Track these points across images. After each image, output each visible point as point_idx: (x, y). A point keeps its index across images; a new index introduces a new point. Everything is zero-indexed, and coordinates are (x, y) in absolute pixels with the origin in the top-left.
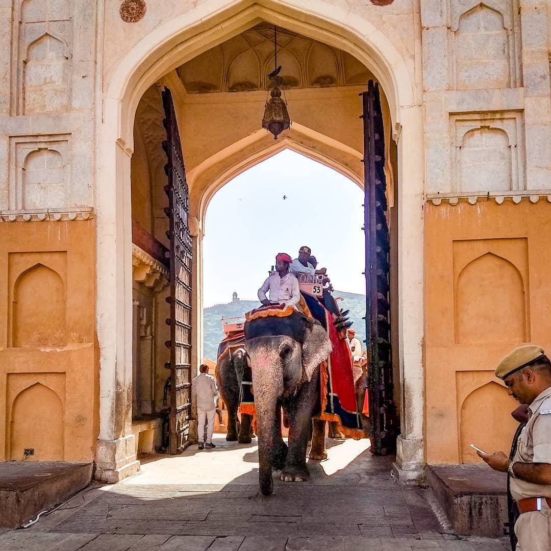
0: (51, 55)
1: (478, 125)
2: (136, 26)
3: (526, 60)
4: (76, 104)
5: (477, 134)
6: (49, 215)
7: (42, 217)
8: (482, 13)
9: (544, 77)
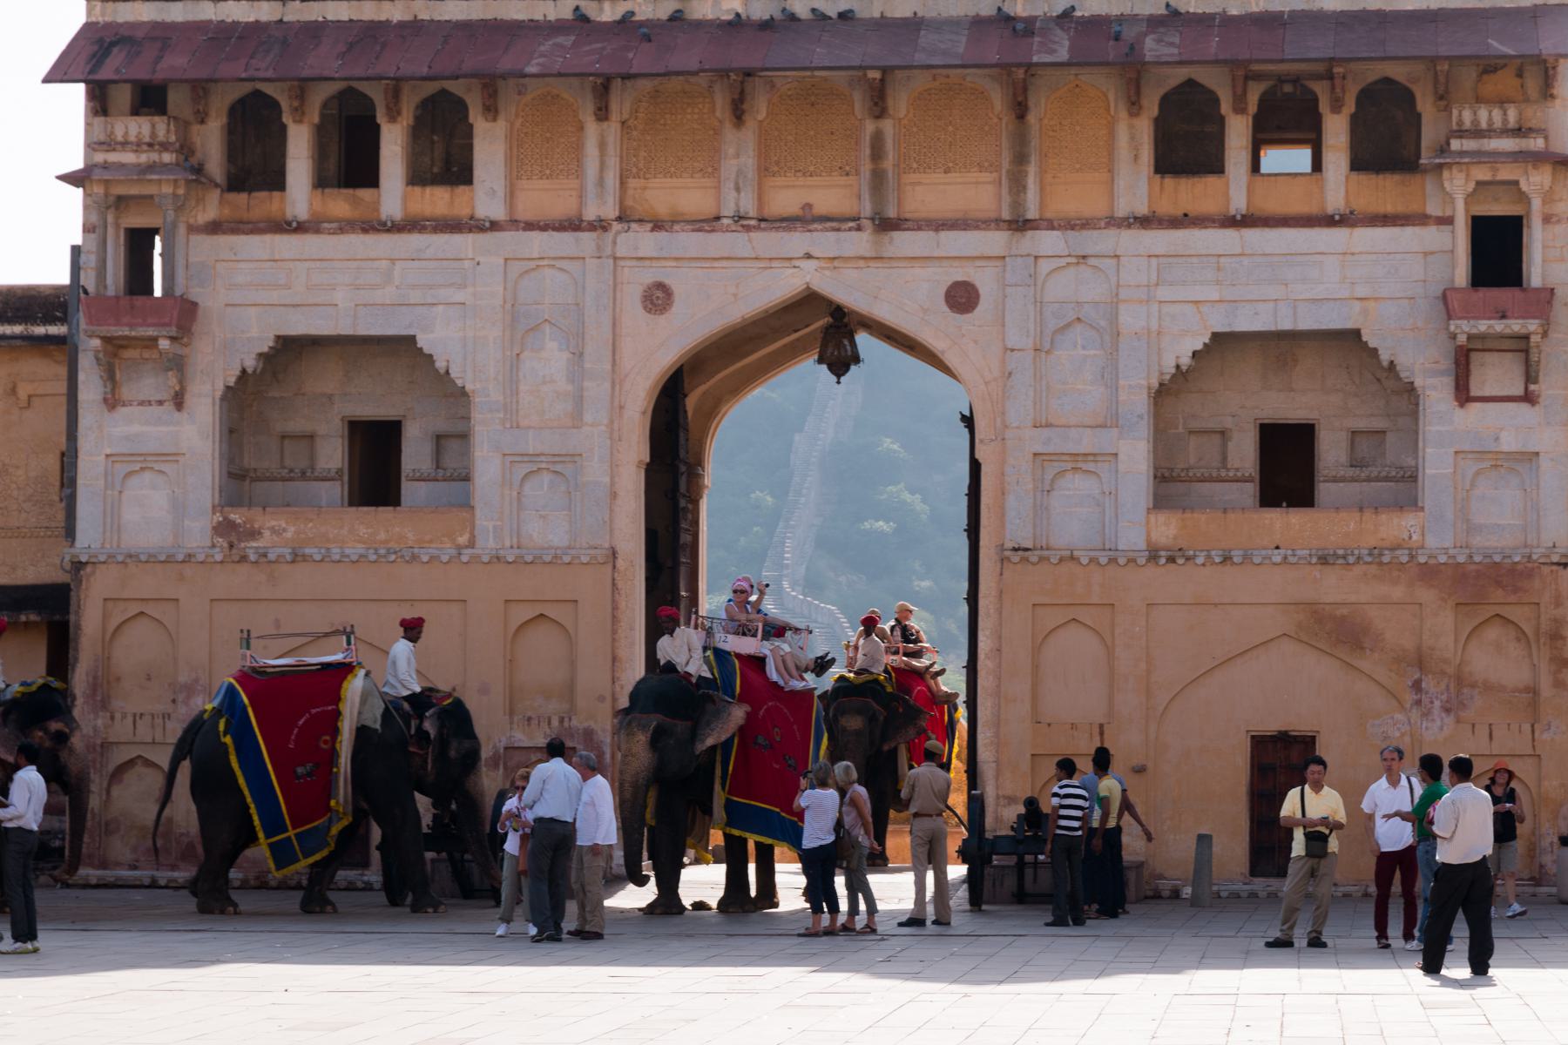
0: (551, 345)
1: (1069, 466)
2: (662, 320)
3: (1123, 397)
4: (588, 418)
5: (1069, 476)
6: (556, 557)
7: (548, 558)
8: (1079, 328)
9: (1140, 417)
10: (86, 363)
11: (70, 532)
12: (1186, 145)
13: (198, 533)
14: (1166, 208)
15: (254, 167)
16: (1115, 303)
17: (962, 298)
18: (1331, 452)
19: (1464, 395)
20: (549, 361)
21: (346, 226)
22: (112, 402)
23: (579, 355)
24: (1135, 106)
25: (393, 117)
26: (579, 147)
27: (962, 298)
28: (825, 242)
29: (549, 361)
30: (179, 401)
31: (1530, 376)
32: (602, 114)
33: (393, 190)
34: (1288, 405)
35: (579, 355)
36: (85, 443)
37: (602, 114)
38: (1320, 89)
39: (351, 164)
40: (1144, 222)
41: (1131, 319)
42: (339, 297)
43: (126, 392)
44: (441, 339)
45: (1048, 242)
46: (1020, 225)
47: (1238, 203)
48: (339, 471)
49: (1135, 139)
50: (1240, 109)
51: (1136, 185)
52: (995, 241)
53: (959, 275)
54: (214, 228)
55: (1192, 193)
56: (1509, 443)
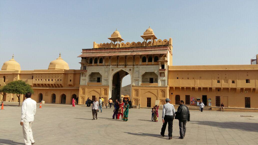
10: (81, 75)
11: (80, 84)
12: (144, 60)
13: (86, 84)
14: (142, 64)
15: (91, 62)
16: (139, 70)
17: (130, 70)
18: (154, 80)
19: (161, 76)
20: (106, 74)
21: (95, 66)
22: (82, 76)
23: (108, 73)
24: (141, 58)
25: (98, 59)
26: (109, 60)
27: (130, 70)
28: (122, 66)
29: (106, 74)
30: (86, 76)
31: (165, 75)
32: (110, 59)
33: (98, 63)
34: (152, 77)
35: (108, 73)
36: (81, 79)
37: (110, 59)
38: (152, 57)
39: (96, 62)
40: (141, 65)
41: (140, 71)
42: (95, 70)
43: (83, 75)
44: (100, 72)
45: (135, 66)
46: (134, 65)
47: (147, 64)
48: (96, 81)
49: (141, 60)
50: (147, 58)
51: (141, 63)
52: (132, 66)
53: (130, 68)
54: (88, 66)
55: (144, 63)
56: (163, 79)
